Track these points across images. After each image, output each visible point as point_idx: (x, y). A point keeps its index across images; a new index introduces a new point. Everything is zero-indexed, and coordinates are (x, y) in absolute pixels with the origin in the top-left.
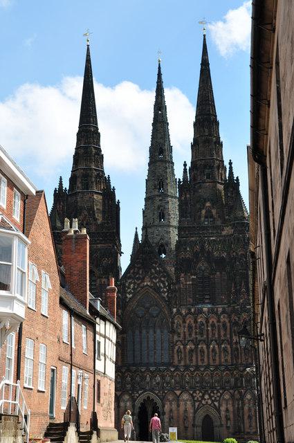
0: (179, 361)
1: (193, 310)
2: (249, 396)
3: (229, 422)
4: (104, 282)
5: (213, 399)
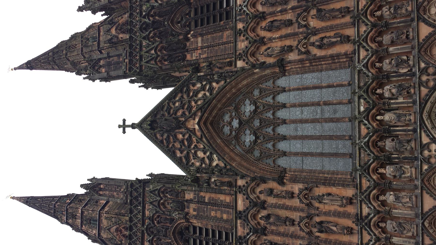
0: (347, 39)
4: (194, 210)
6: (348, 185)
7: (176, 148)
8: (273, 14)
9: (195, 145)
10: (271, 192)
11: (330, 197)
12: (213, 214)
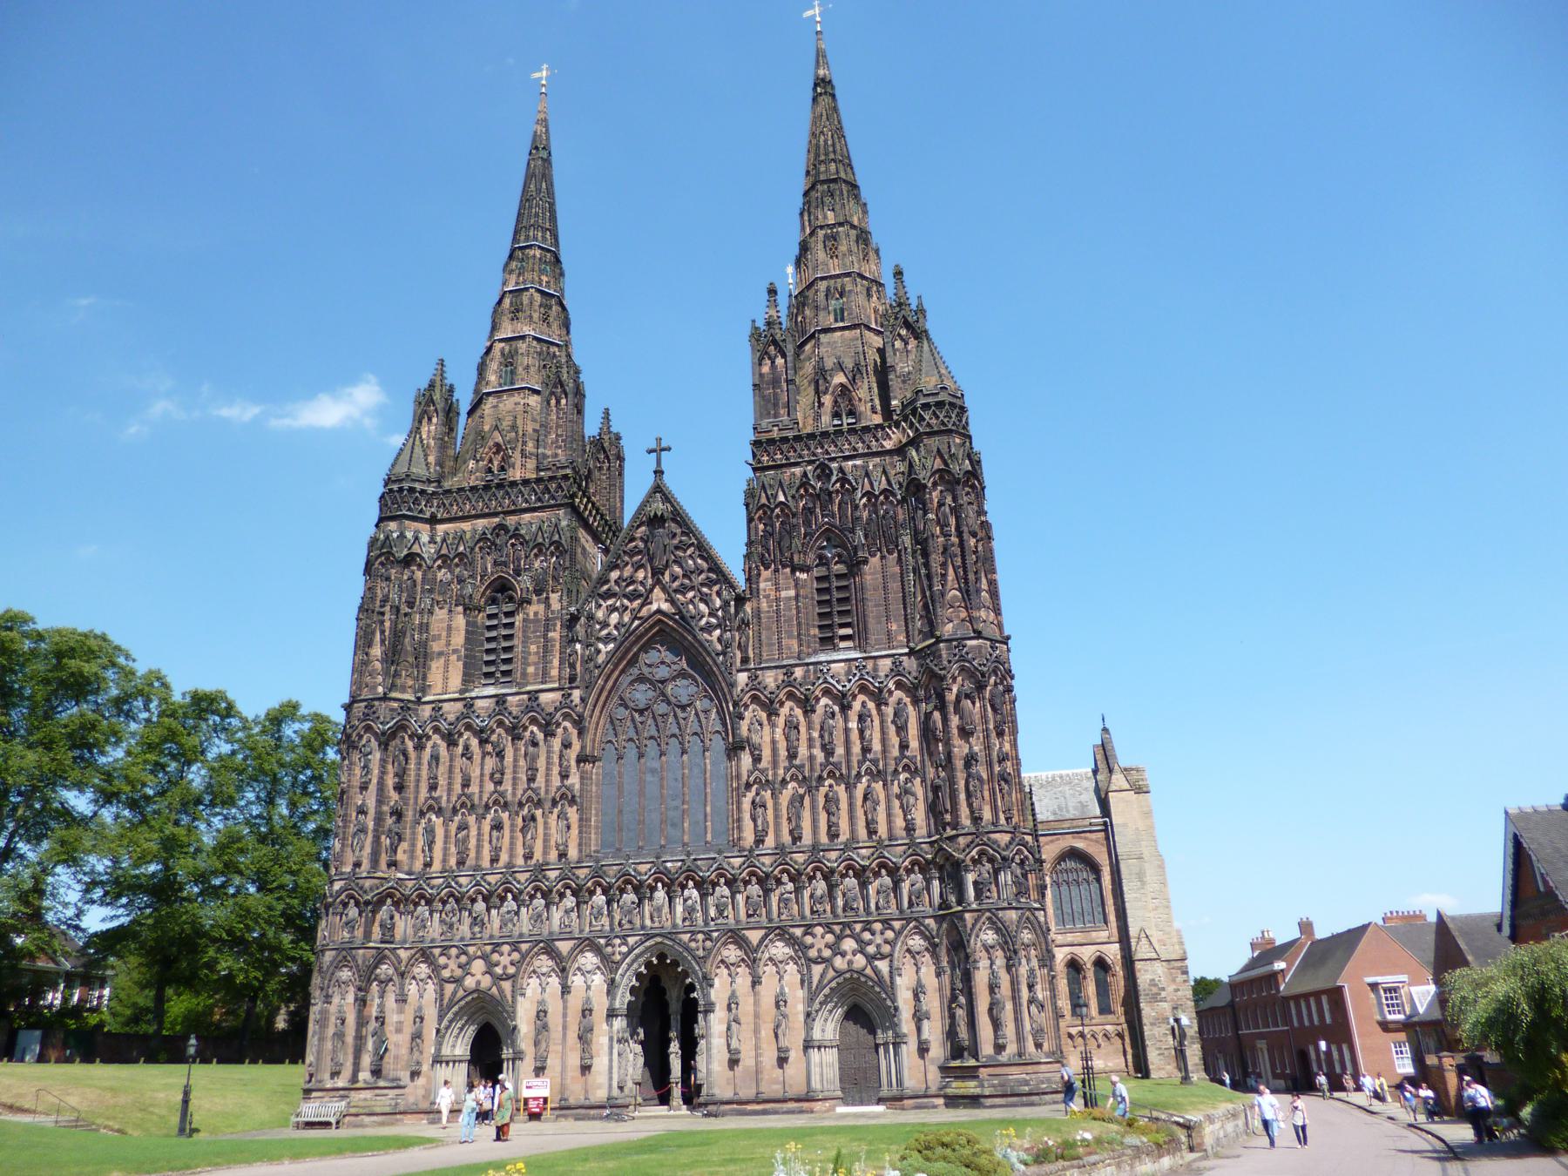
1: (799, 673)
2: (990, 937)
3: (926, 1024)
4: (536, 614)
5: (871, 949)
6: (580, 851)
7: (622, 570)
8: (810, 727)
9: (627, 608)
10: (567, 745)
11: (565, 829)
12: (533, 648)
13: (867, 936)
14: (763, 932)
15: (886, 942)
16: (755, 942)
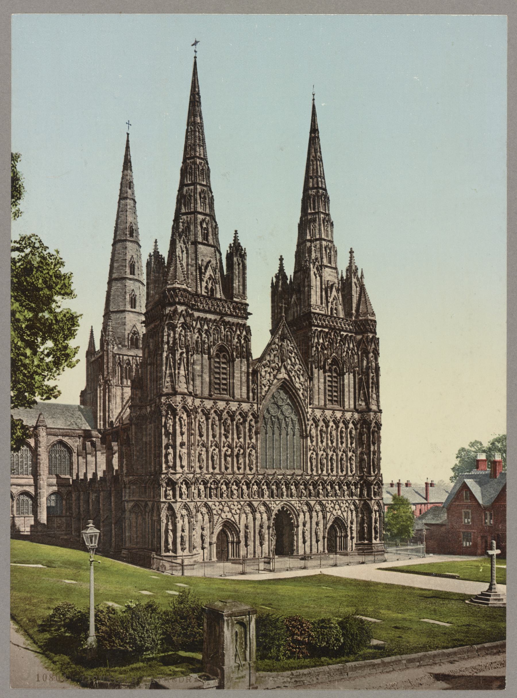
13: (342, 505)
14: (315, 502)
15: (346, 506)
16: (312, 505)
